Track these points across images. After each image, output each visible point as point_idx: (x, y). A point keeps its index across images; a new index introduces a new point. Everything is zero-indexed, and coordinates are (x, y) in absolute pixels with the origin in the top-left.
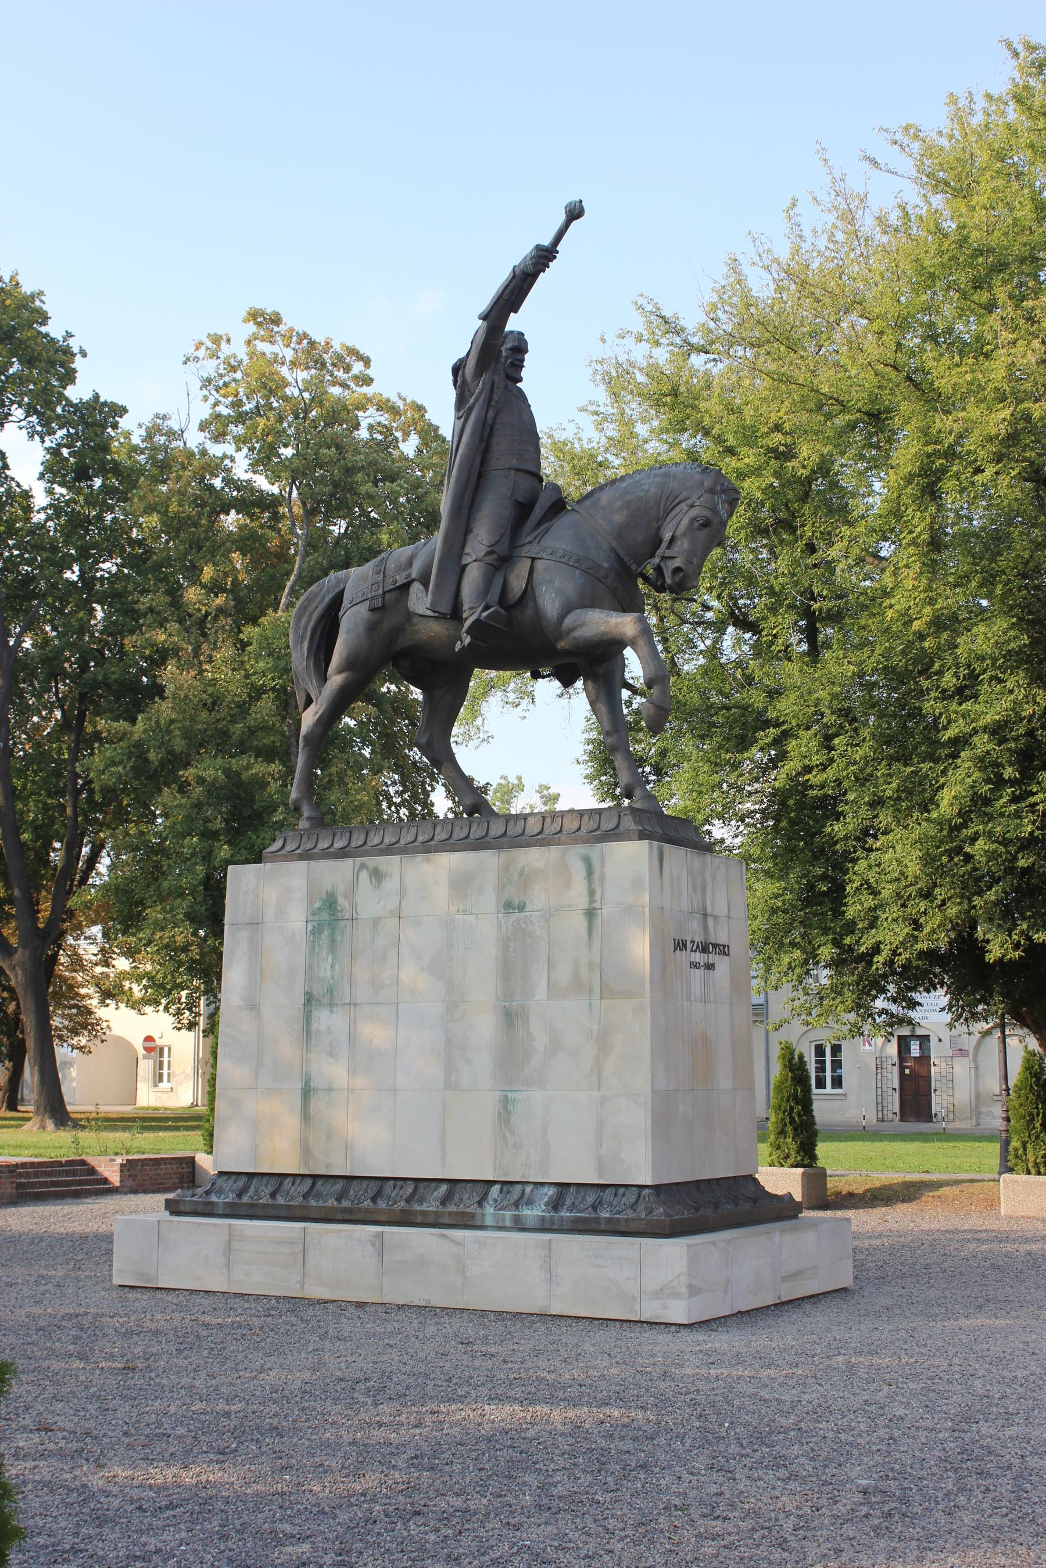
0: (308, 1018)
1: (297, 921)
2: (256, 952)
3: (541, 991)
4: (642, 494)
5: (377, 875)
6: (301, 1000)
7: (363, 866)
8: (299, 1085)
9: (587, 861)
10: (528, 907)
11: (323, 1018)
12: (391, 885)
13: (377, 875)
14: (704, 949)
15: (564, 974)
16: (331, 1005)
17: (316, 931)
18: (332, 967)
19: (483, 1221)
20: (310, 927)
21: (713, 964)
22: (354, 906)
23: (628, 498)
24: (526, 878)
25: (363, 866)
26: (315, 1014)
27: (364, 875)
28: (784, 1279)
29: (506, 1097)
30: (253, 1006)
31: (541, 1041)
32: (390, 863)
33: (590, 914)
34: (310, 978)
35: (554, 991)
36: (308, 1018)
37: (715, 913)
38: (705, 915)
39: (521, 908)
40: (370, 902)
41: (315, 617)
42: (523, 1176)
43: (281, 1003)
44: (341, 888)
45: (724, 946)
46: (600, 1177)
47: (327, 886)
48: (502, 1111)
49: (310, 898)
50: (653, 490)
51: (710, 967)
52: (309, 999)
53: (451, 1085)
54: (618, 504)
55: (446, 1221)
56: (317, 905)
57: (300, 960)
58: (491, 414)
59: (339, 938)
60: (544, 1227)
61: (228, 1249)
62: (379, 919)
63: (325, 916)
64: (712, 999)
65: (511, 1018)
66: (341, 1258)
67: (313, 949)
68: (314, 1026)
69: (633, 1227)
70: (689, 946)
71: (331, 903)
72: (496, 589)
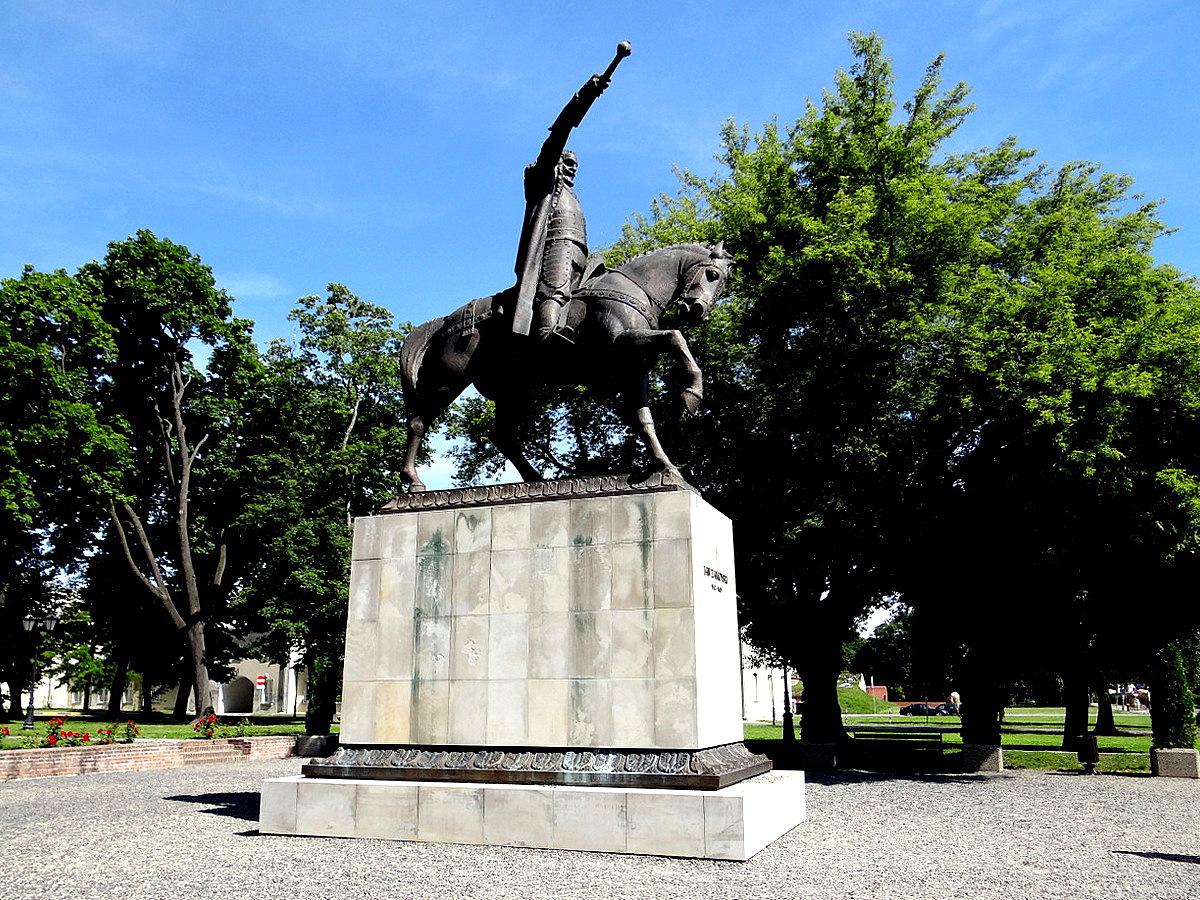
0: (418, 627)
1: (410, 554)
2: (376, 580)
3: (606, 604)
5: (473, 521)
7: (461, 514)
11: (429, 627)
12: (484, 527)
13: (473, 521)
15: (624, 589)
16: (436, 617)
17: (424, 564)
19: (563, 779)
20: (419, 561)
22: (455, 543)
24: (593, 519)
25: (461, 514)
26: (423, 624)
27: (462, 521)
29: (577, 683)
30: (373, 619)
31: (606, 640)
33: (645, 545)
35: (616, 604)
36: (418, 627)
39: (589, 542)
40: (466, 540)
42: (592, 744)
43: (396, 616)
44: (445, 531)
47: (433, 529)
48: (574, 694)
49: (420, 539)
52: (418, 613)
53: (531, 676)
55: (533, 779)
56: (426, 544)
57: (412, 583)
61: (355, 805)
62: (475, 553)
65: (582, 622)
71: (437, 542)
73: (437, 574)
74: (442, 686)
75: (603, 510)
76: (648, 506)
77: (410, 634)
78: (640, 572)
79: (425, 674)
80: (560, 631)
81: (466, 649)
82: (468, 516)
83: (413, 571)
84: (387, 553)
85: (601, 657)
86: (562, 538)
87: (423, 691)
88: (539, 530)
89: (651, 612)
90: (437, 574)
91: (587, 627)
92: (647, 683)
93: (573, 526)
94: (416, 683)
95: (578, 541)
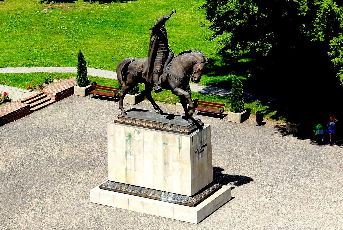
0: (126, 156)
4: (189, 60)
6: (125, 152)
8: (125, 168)
9: (179, 139)
10: (168, 145)
11: (129, 156)
13: (139, 132)
16: (131, 154)
17: (127, 140)
18: (130, 147)
22: (134, 137)
23: (186, 61)
32: (141, 130)
33: (180, 148)
34: (126, 148)
36: (126, 156)
41: (122, 69)
43: (121, 152)
44: (131, 133)
46: (182, 194)
49: (125, 134)
50: (191, 59)
51: (202, 151)
52: (126, 152)
54: (184, 62)
56: (127, 135)
59: (131, 142)
60: (172, 202)
62: (139, 140)
63: (128, 138)
65: (165, 163)
66: (135, 203)
67: (126, 143)
68: (127, 158)
69: (188, 205)
71: (130, 136)
72: (160, 80)
73: (130, 144)
75: (170, 137)
76: (181, 140)
77: (124, 157)
78: (179, 154)
79: (128, 168)
80: (161, 164)
82: (137, 130)
84: (117, 135)
86: (160, 142)
87: (128, 171)
88: (155, 138)
89: (181, 164)
90: (130, 144)
91: (167, 164)
92: (180, 180)
93: (163, 140)
94: (126, 169)
95: (164, 143)
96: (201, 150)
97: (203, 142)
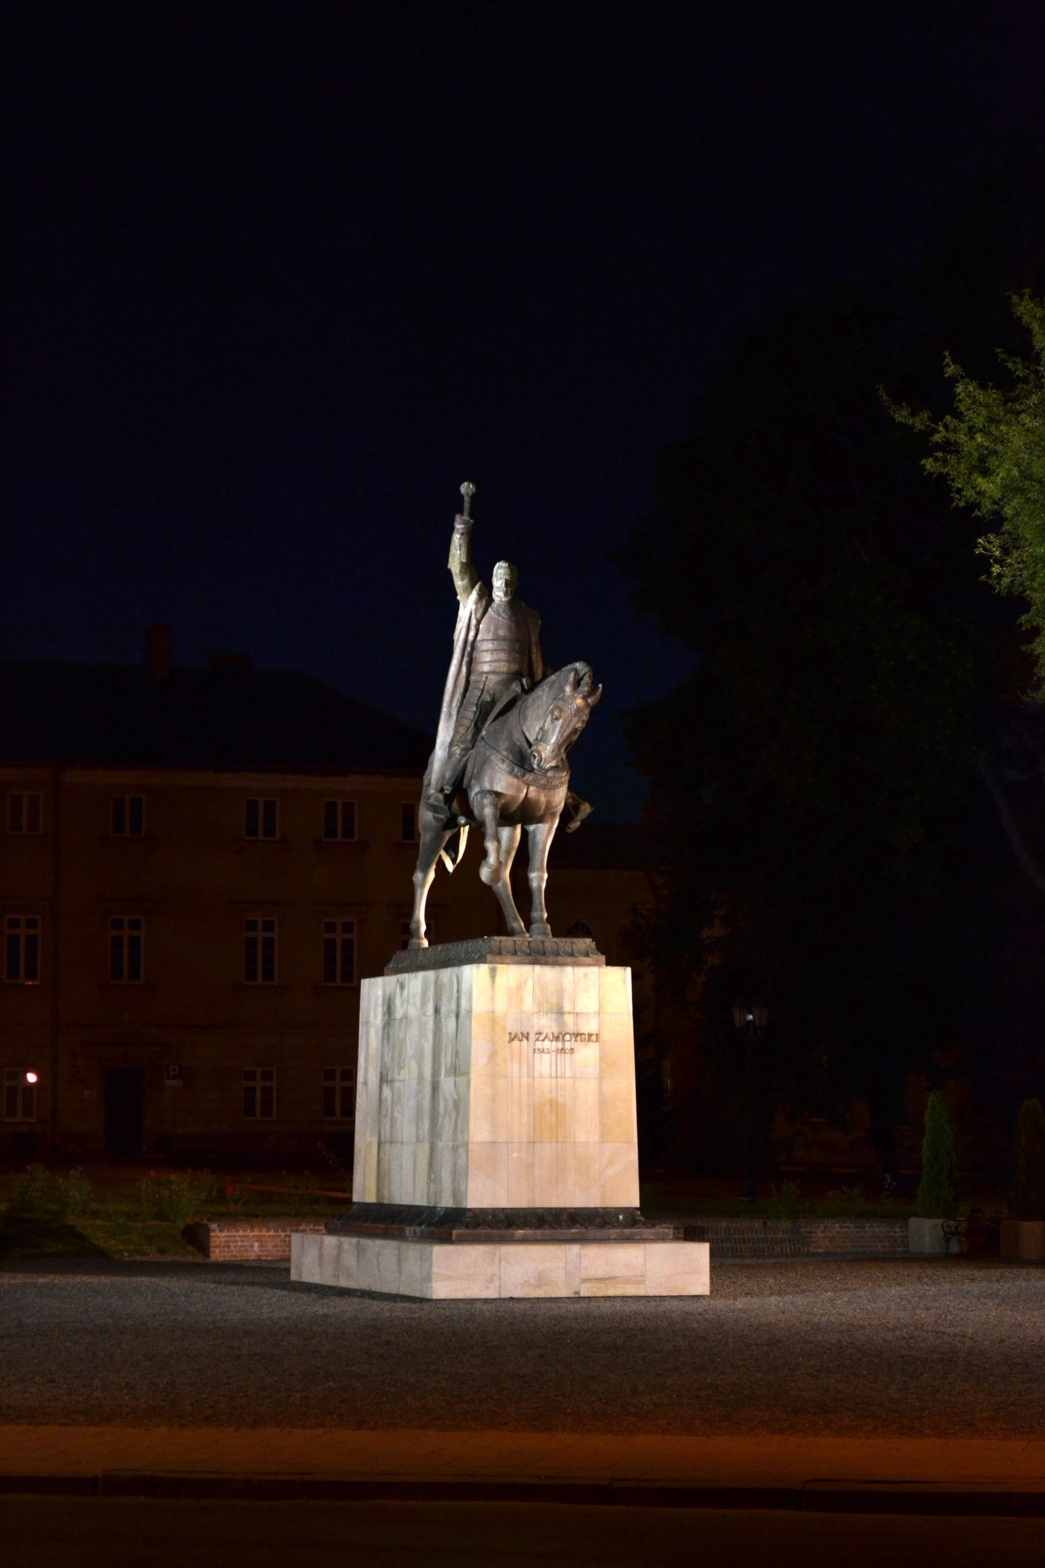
5: (402, 987)
14: (557, 1039)
17: (384, 1029)
21: (572, 1049)
28: (585, 1280)
33: (457, 1016)
34: (382, 1061)
37: (578, 1010)
38: (560, 1013)
45: (590, 1035)
51: (563, 1050)
53: (418, 1139)
57: (380, 1046)
58: (472, 634)
64: (568, 1074)
70: (532, 1037)
74: (388, 1145)
79: (383, 1139)
81: (396, 1114)
83: (380, 1033)
85: (440, 1119)
94: (379, 1144)
96: (555, 1045)
97: (569, 1019)
